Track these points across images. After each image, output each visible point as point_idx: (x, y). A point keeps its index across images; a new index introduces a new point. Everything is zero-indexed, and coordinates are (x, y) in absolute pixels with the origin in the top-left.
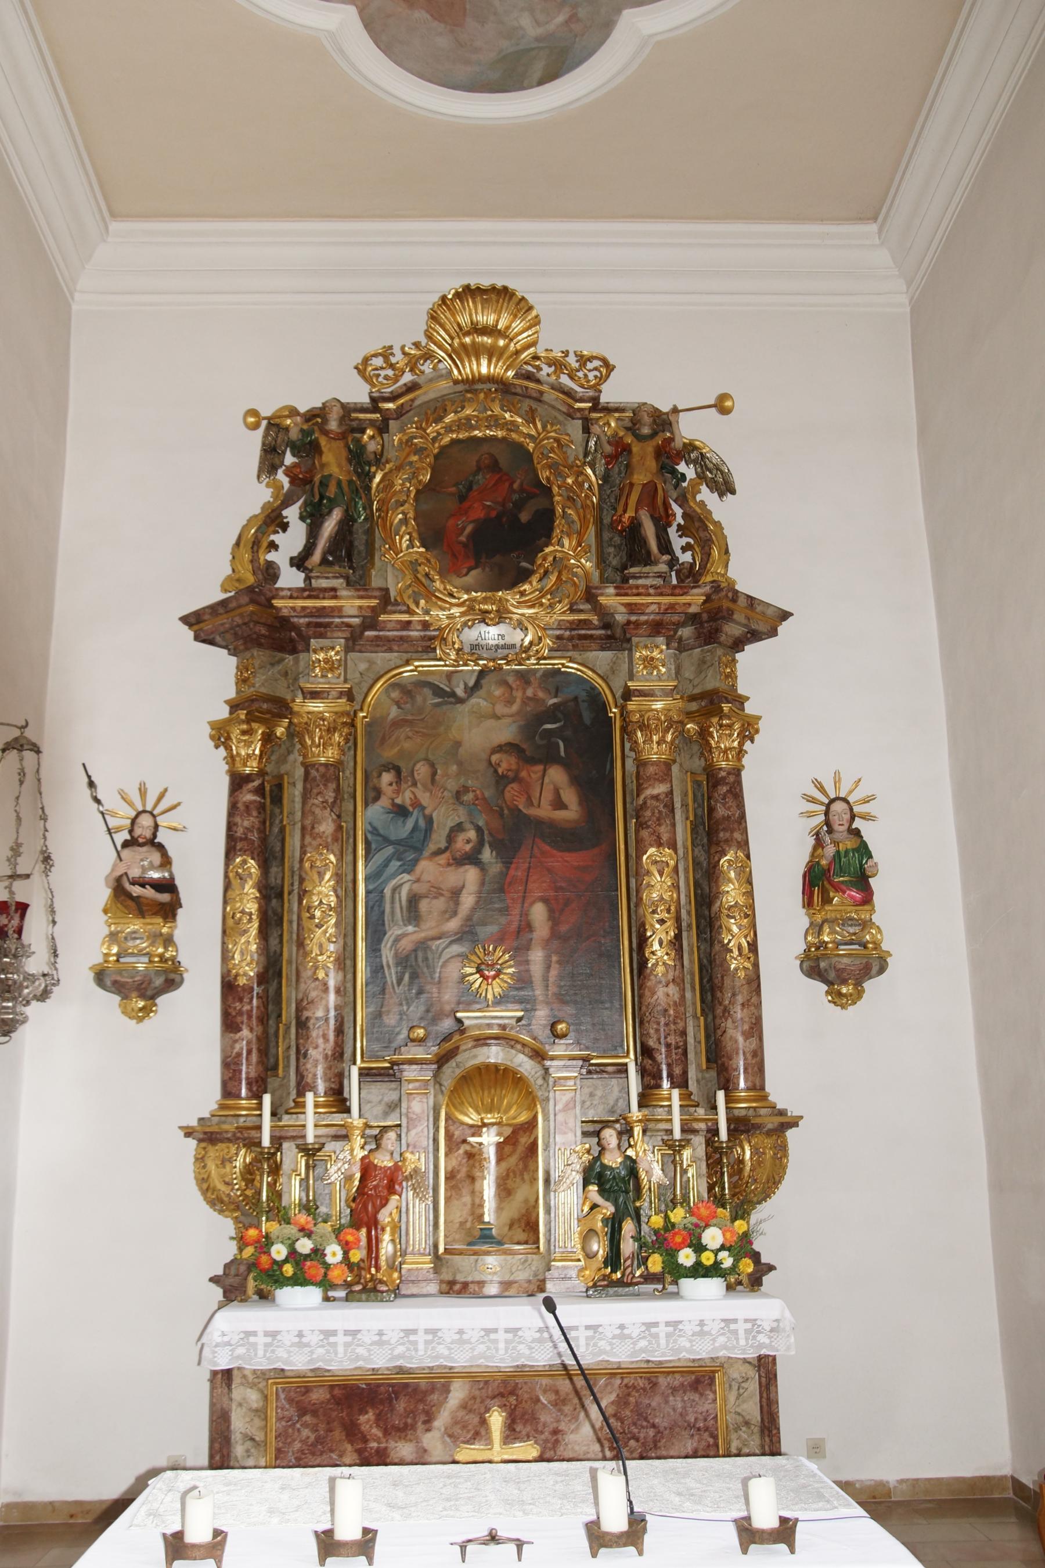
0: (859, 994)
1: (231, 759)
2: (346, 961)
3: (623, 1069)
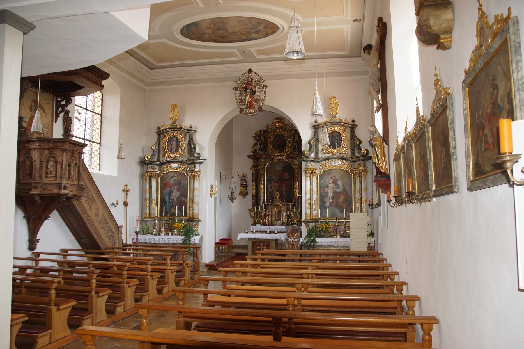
2: (264, 193)
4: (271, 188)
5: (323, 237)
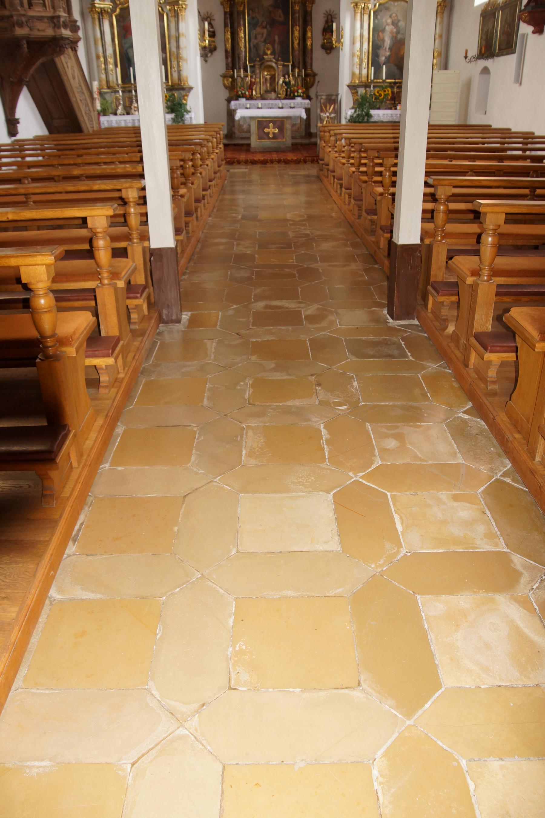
0: (330, 52)
1: (224, 8)
3: (289, 66)
4: (256, 38)
5: (379, 109)
